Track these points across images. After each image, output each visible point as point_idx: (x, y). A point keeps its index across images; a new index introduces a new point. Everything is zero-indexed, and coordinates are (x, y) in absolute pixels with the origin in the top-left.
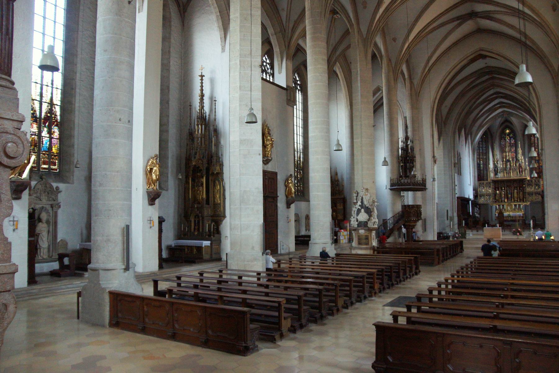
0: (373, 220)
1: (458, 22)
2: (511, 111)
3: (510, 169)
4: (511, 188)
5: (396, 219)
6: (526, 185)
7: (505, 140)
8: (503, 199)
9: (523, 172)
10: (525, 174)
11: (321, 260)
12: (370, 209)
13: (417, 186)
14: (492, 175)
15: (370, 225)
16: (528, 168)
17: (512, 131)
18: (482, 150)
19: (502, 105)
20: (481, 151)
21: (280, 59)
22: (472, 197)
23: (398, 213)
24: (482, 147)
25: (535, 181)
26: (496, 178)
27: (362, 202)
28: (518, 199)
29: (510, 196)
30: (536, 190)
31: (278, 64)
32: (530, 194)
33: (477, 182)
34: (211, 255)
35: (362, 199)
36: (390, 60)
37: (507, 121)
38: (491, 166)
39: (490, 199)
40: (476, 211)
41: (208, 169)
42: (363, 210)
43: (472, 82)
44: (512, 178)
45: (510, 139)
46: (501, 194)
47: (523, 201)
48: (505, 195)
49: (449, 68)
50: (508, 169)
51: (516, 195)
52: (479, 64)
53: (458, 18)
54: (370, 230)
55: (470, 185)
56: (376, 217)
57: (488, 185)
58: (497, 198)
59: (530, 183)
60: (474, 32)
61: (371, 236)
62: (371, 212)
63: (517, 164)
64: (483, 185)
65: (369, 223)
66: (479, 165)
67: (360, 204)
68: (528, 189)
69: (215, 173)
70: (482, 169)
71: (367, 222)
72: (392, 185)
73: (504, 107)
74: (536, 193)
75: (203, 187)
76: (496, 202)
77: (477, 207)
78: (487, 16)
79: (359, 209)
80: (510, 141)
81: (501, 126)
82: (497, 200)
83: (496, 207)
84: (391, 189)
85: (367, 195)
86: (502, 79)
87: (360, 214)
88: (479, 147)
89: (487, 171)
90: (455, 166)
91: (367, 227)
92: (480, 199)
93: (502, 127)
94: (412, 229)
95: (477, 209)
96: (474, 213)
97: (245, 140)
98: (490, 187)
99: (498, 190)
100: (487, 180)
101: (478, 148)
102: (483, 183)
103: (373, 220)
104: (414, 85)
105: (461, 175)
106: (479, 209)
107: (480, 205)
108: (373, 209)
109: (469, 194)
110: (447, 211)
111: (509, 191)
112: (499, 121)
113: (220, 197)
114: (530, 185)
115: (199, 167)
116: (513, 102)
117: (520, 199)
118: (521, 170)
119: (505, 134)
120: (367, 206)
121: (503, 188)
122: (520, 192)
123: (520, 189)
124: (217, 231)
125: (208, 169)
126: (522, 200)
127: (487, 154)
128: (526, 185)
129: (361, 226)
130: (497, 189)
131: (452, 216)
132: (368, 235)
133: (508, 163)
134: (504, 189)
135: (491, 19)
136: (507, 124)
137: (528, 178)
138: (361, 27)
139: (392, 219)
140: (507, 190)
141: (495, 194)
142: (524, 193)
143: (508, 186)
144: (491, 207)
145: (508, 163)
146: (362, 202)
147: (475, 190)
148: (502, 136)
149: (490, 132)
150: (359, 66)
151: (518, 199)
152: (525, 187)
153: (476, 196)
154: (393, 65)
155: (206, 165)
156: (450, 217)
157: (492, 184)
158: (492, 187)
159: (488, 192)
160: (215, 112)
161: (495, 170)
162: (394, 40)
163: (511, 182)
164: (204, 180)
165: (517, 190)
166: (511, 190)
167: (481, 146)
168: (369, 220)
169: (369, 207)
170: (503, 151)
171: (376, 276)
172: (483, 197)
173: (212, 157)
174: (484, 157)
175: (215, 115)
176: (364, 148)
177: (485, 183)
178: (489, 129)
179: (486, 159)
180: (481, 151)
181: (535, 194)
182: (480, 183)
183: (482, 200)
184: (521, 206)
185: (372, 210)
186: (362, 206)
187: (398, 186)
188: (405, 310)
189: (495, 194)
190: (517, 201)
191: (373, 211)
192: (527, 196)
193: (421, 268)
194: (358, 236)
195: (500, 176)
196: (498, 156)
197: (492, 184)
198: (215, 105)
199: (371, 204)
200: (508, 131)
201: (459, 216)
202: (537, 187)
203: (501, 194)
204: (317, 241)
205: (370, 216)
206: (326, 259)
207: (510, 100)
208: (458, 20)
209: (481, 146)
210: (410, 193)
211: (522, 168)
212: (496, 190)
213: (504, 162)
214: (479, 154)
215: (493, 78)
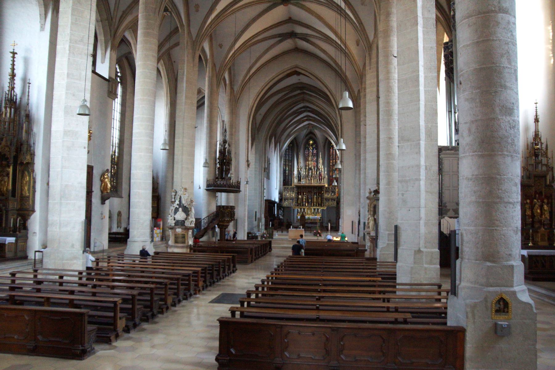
0: (191, 220)
1: (279, 39)
2: (315, 124)
5: (210, 219)
7: (309, 149)
8: (304, 203)
10: (324, 181)
11: (141, 259)
12: (187, 208)
13: (232, 188)
14: (296, 181)
15: (187, 224)
16: (326, 176)
17: (315, 142)
18: (289, 157)
19: (308, 118)
20: (287, 158)
21: (104, 48)
22: (277, 200)
23: (213, 213)
25: (332, 189)
26: (299, 183)
27: (180, 201)
29: (310, 200)
30: (332, 197)
31: (102, 54)
32: (327, 200)
33: (282, 186)
34: (16, 252)
35: (180, 198)
36: (214, 65)
37: (311, 133)
38: (296, 172)
41: (16, 158)
43: (285, 95)
44: (313, 185)
45: (313, 149)
46: (302, 198)
47: (321, 206)
48: (306, 199)
49: (267, 79)
51: (315, 200)
52: (294, 80)
53: (280, 35)
54: (187, 229)
55: (277, 189)
56: (193, 216)
57: (292, 190)
58: (299, 202)
59: (327, 190)
60: (292, 50)
61: (188, 234)
62: (189, 211)
63: (318, 173)
65: (186, 222)
66: (285, 171)
67: (178, 203)
68: (326, 196)
69: (25, 162)
70: (287, 174)
71: (184, 221)
72: (208, 186)
73: (310, 120)
74: (333, 199)
75: (9, 177)
76: (298, 205)
77: (281, 210)
78: (304, 37)
80: (313, 151)
83: (298, 210)
84: (207, 190)
86: (311, 96)
87: (178, 213)
88: (286, 155)
89: (291, 176)
90: (265, 171)
92: (284, 202)
93: (307, 137)
94: (225, 229)
97: (69, 131)
98: (293, 192)
99: (301, 195)
100: (291, 185)
102: (288, 188)
103: (191, 220)
104: (234, 91)
105: (269, 179)
106: (283, 211)
107: (284, 208)
108: (191, 208)
109: (275, 197)
110: (256, 212)
112: (305, 132)
113: (29, 190)
114: (328, 192)
115: (5, 155)
116: (319, 117)
117: (318, 204)
119: (309, 144)
120: (185, 205)
123: (319, 195)
124: (24, 227)
125: (16, 158)
126: (320, 205)
127: (292, 161)
128: (324, 192)
129: (178, 225)
131: (259, 217)
133: (310, 171)
135: (308, 41)
136: (311, 135)
137: (326, 186)
138: (191, 29)
139: (207, 219)
141: (298, 199)
142: (322, 199)
143: (309, 192)
144: (294, 210)
145: (310, 171)
146: (180, 201)
147: (280, 193)
148: (306, 147)
149: (296, 141)
150: (185, 68)
153: (281, 199)
154: (217, 70)
155: (13, 154)
156: (259, 219)
157: (295, 189)
160: (28, 96)
161: (298, 177)
162: (221, 46)
164: (11, 170)
165: (316, 195)
167: (287, 153)
168: (186, 219)
169: (187, 206)
170: (306, 159)
171: (200, 275)
173: (21, 145)
174: (290, 164)
175: (28, 99)
176: (185, 148)
178: (295, 139)
179: (291, 166)
180: (287, 158)
182: (285, 188)
183: (285, 204)
184: (319, 210)
185: (189, 209)
186: (180, 205)
187: (214, 187)
188: (239, 306)
189: (298, 199)
190: (316, 205)
192: (325, 201)
193: (238, 266)
194: (175, 235)
195: (303, 182)
196: (302, 164)
197: (295, 189)
198: (29, 88)
200: (311, 142)
201: (265, 217)
203: (302, 198)
204: (136, 239)
205: (188, 215)
206: (146, 257)
207: (316, 115)
208: (279, 37)
209: (287, 153)
210: (224, 195)
211: (321, 176)
212: (298, 195)
213: (307, 170)
214: (285, 161)
215: (304, 93)
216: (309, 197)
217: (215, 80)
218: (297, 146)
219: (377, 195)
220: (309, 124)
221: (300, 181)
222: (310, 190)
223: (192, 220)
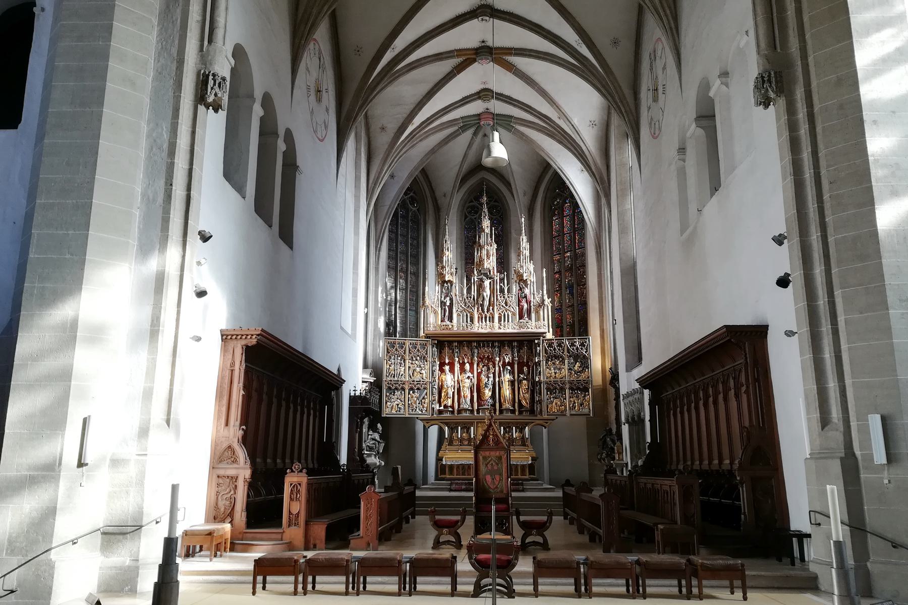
3: (491, 304)
4: (494, 367)
6: (542, 358)
9: (533, 315)
16: (547, 301)
24: (405, 236)
25: (573, 345)
28: (514, 406)
30: (574, 377)
32: (556, 388)
39: (420, 403)
40: (367, 443)
50: (486, 303)
64: (401, 351)
81: (464, 180)
82: (445, 406)
95: (377, 436)
96: (361, 449)
98: (424, 358)
101: (393, 236)
102: (402, 346)
105: (286, 235)
111: (488, 377)
114: (557, 357)
118: (526, 306)
121: (467, 366)
122: (520, 382)
123: (520, 371)
128: (542, 358)
130: (447, 368)
134: (472, 371)
137: (550, 336)
140: (479, 374)
151: (514, 406)
152: (539, 362)
158: (430, 359)
159: (417, 377)
161: (443, 304)
163: (493, 347)
165: (512, 372)
166: (494, 374)
172: (398, 393)
177: (408, 343)
179: (416, 274)
181: (571, 389)
183: (392, 407)
192: (545, 395)
195: (457, 325)
197: (429, 348)
202: (576, 368)
211: (529, 302)
216: (484, 378)
218: (437, 209)
220: (484, 94)
221: (451, 319)
222: (486, 351)
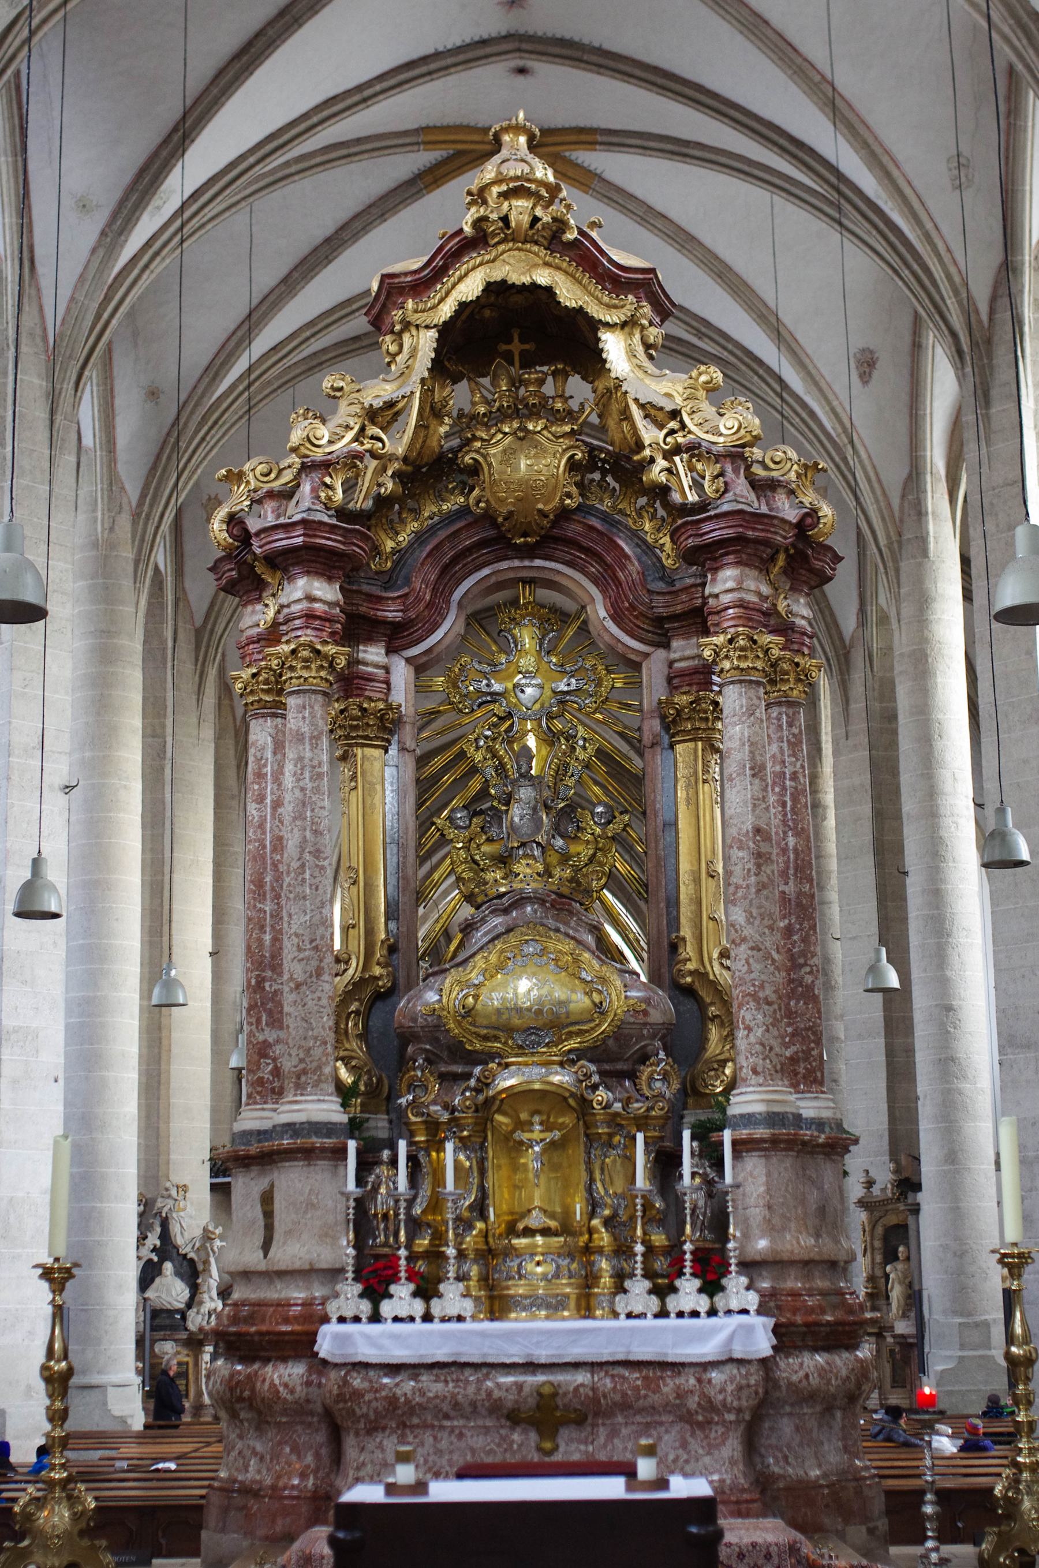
12: (192, 1260)
27: (165, 1236)
42: (168, 1267)
65: (191, 1313)
67: (158, 1243)
79: (150, 1261)
85: (184, 1210)
91: (186, 1329)
108: (206, 1262)
132: (186, 1359)
138: (188, 584)
168: (189, 1305)
169: (192, 1255)
185: (200, 1267)
191: (207, 1270)
199: (197, 1245)
205: (195, 1289)
217: (232, 752)
219: (910, 1195)
223: (213, 1305)
